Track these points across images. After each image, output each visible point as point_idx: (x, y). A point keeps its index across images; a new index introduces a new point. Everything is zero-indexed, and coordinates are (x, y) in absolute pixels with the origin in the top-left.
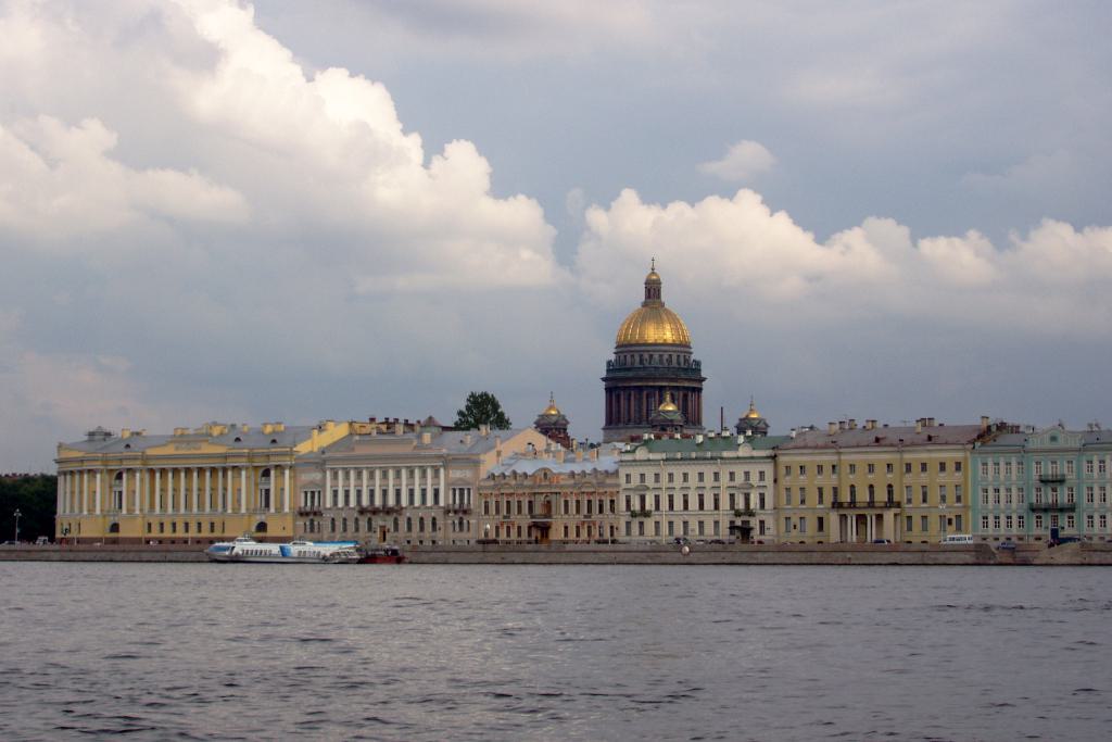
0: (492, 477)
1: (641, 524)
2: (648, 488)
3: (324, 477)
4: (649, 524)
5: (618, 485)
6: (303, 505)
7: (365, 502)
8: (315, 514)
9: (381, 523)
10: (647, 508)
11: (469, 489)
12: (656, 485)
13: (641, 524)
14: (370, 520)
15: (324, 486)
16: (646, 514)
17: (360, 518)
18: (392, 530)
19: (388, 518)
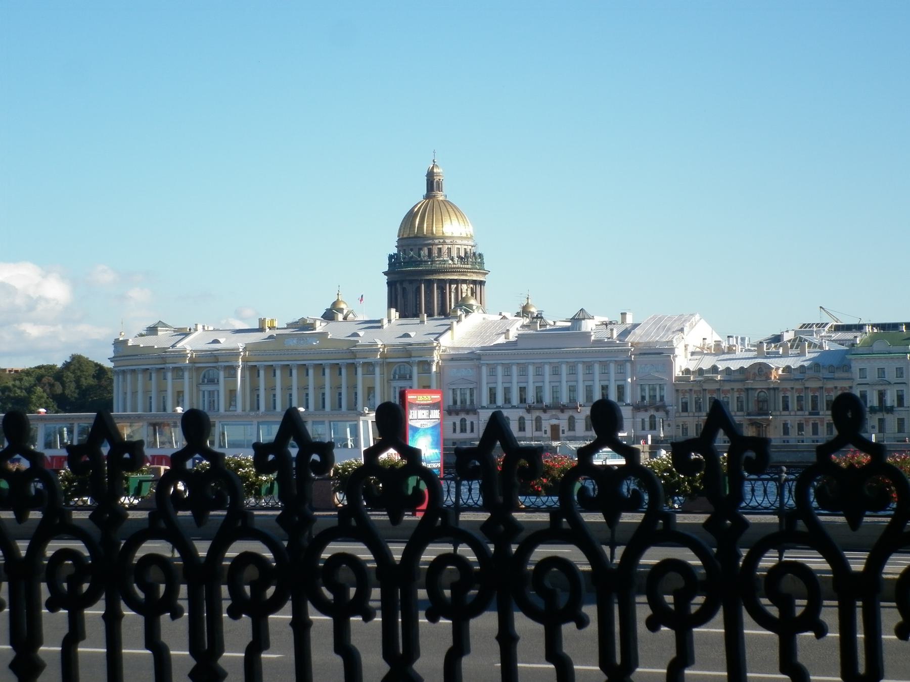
0: (687, 371)
1: (881, 421)
2: (889, 383)
3: (479, 374)
4: (891, 421)
5: (852, 379)
6: (451, 403)
7: (531, 397)
8: (468, 412)
9: (554, 422)
10: (889, 404)
11: (661, 389)
12: (900, 380)
13: (881, 421)
14: (538, 420)
15: (479, 382)
16: (890, 410)
17: (527, 417)
18: (566, 428)
19: (561, 415)
